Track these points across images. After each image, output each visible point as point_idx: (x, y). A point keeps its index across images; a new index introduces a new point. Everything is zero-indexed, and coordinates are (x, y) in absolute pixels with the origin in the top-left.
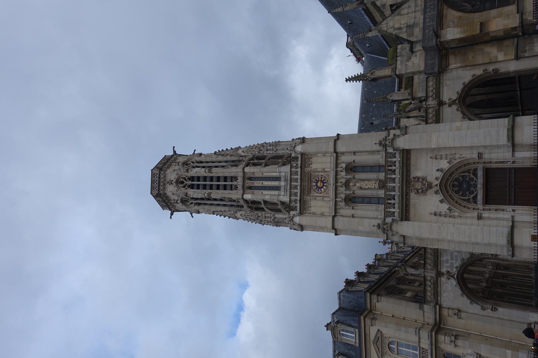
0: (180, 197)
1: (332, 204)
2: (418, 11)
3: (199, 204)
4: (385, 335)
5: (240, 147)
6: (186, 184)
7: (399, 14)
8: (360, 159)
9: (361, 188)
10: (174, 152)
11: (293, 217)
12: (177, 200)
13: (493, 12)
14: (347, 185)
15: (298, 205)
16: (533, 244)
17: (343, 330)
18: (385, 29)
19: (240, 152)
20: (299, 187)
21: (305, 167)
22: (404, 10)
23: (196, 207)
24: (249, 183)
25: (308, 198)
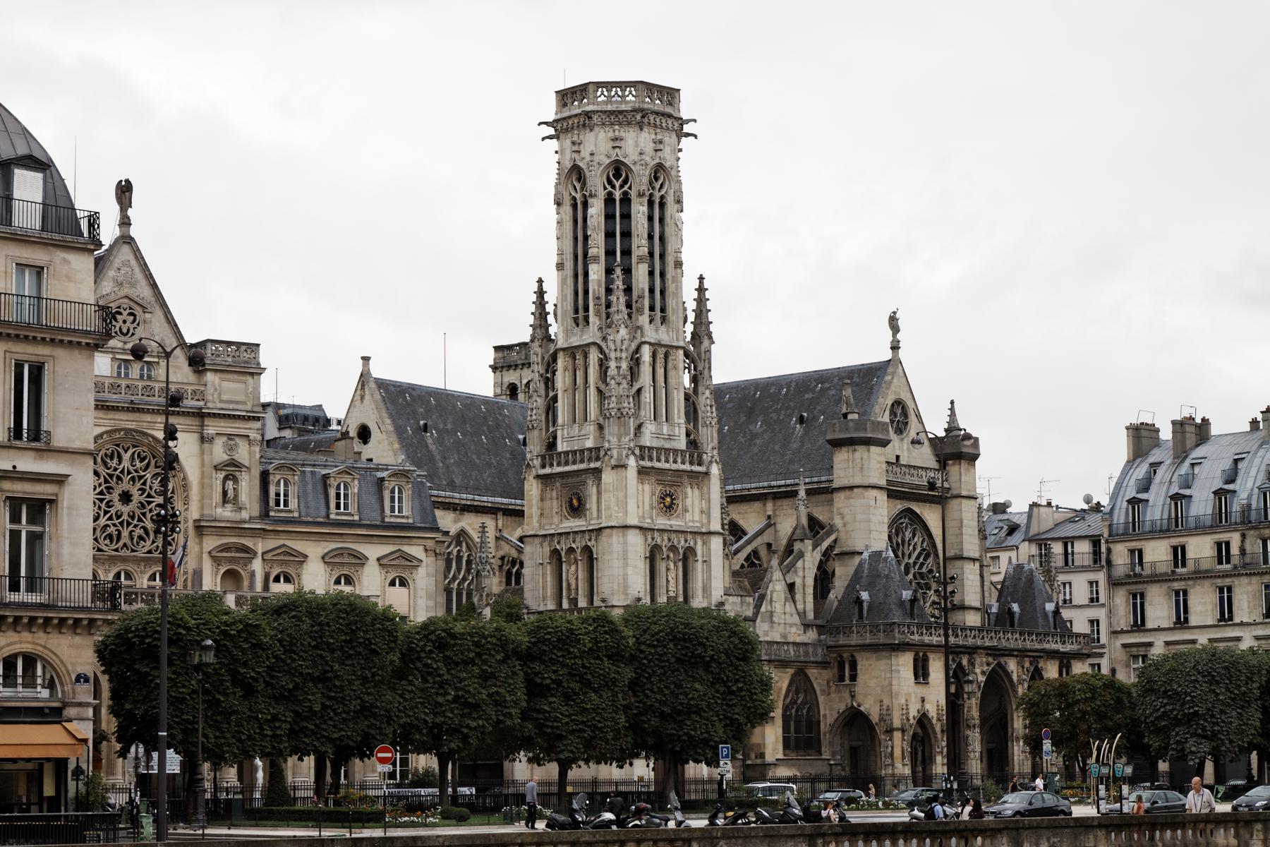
0: (633, 167)
1: (647, 523)
2: (785, 629)
3: (609, 200)
4: (414, 572)
5: (713, 343)
6: (653, 188)
7: (786, 599)
8: (698, 569)
9: (668, 569)
10: (688, 135)
11: (634, 454)
12: (620, 147)
13: (780, 731)
14: (673, 548)
15: (649, 464)
16: (636, 779)
17: (400, 492)
18: (774, 578)
19: (706, 342)
20: (667, 466)
21: (690, 477)
22: (789, 608)
23: (602, 194)
24: (661, 352)
25: (653, 479)
